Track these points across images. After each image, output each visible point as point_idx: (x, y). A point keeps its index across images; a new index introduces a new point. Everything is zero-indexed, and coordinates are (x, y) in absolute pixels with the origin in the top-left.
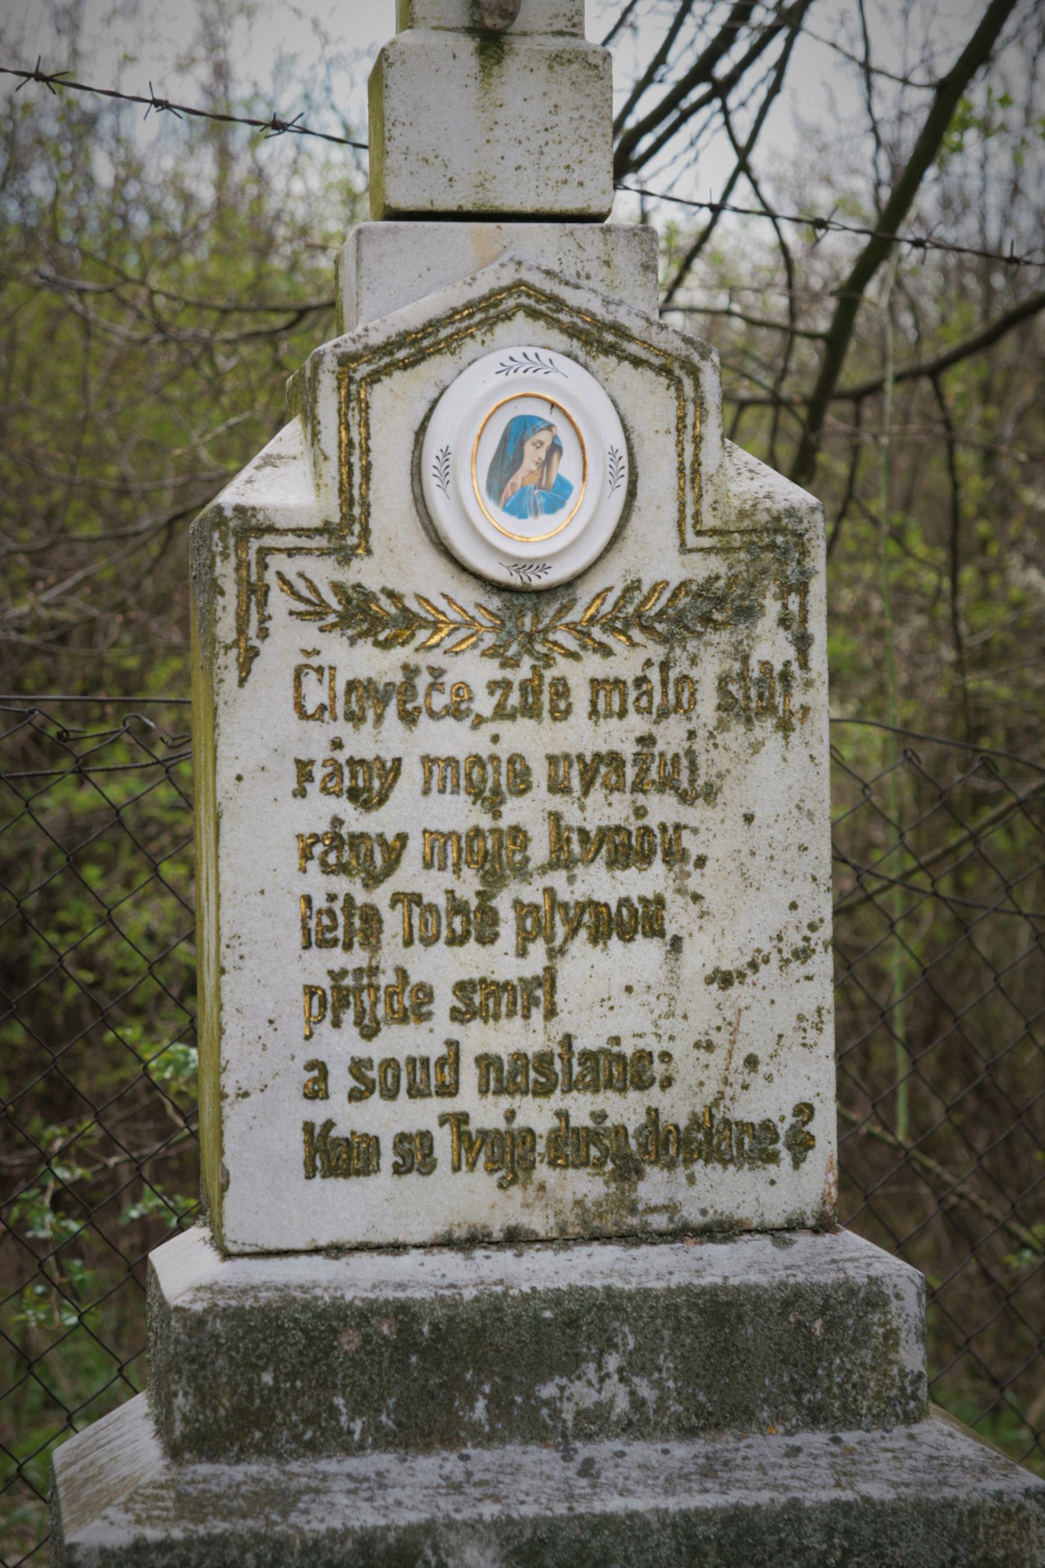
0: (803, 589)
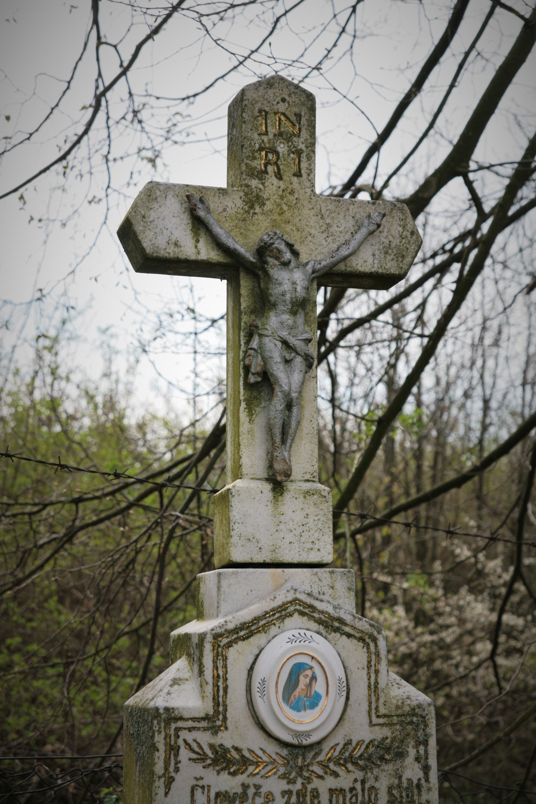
0: (426, 743)
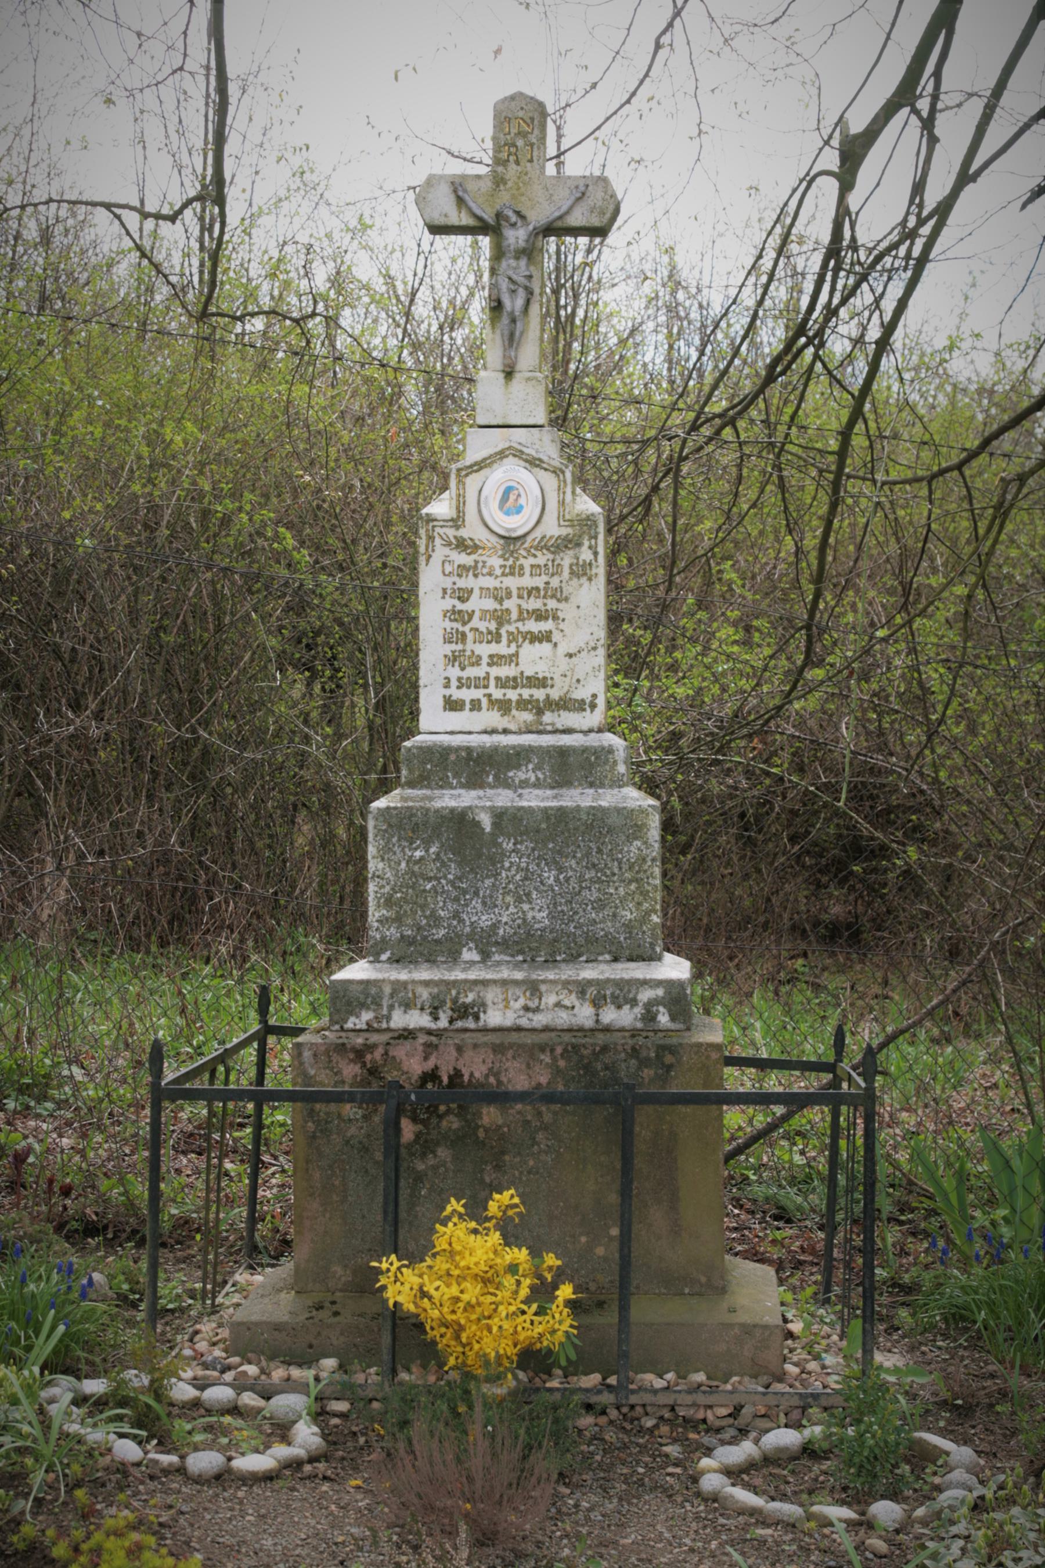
0: (596, 538)
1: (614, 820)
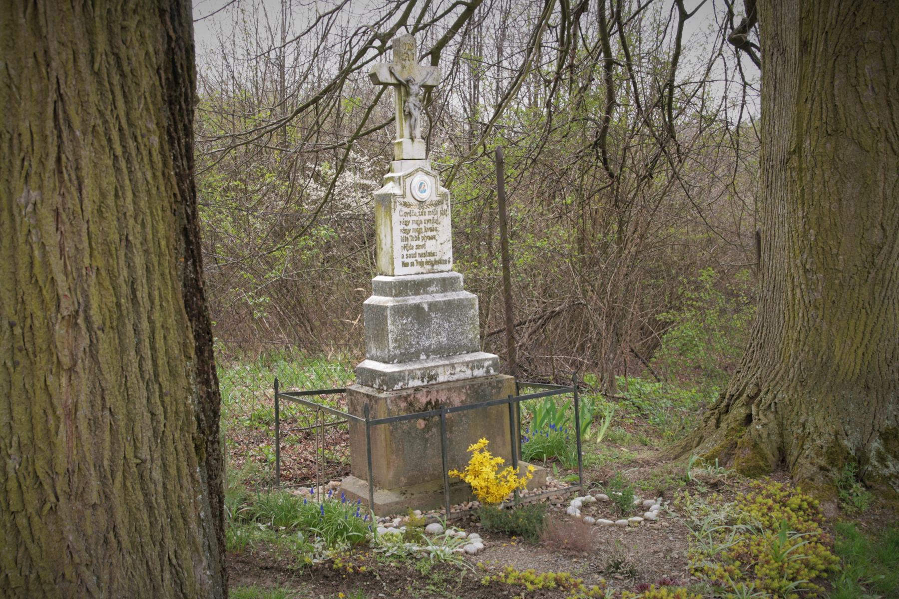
1: (465, 303)
